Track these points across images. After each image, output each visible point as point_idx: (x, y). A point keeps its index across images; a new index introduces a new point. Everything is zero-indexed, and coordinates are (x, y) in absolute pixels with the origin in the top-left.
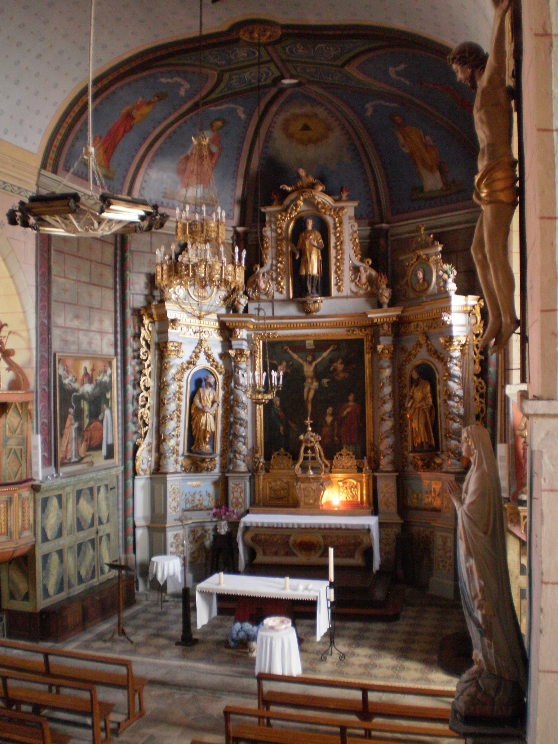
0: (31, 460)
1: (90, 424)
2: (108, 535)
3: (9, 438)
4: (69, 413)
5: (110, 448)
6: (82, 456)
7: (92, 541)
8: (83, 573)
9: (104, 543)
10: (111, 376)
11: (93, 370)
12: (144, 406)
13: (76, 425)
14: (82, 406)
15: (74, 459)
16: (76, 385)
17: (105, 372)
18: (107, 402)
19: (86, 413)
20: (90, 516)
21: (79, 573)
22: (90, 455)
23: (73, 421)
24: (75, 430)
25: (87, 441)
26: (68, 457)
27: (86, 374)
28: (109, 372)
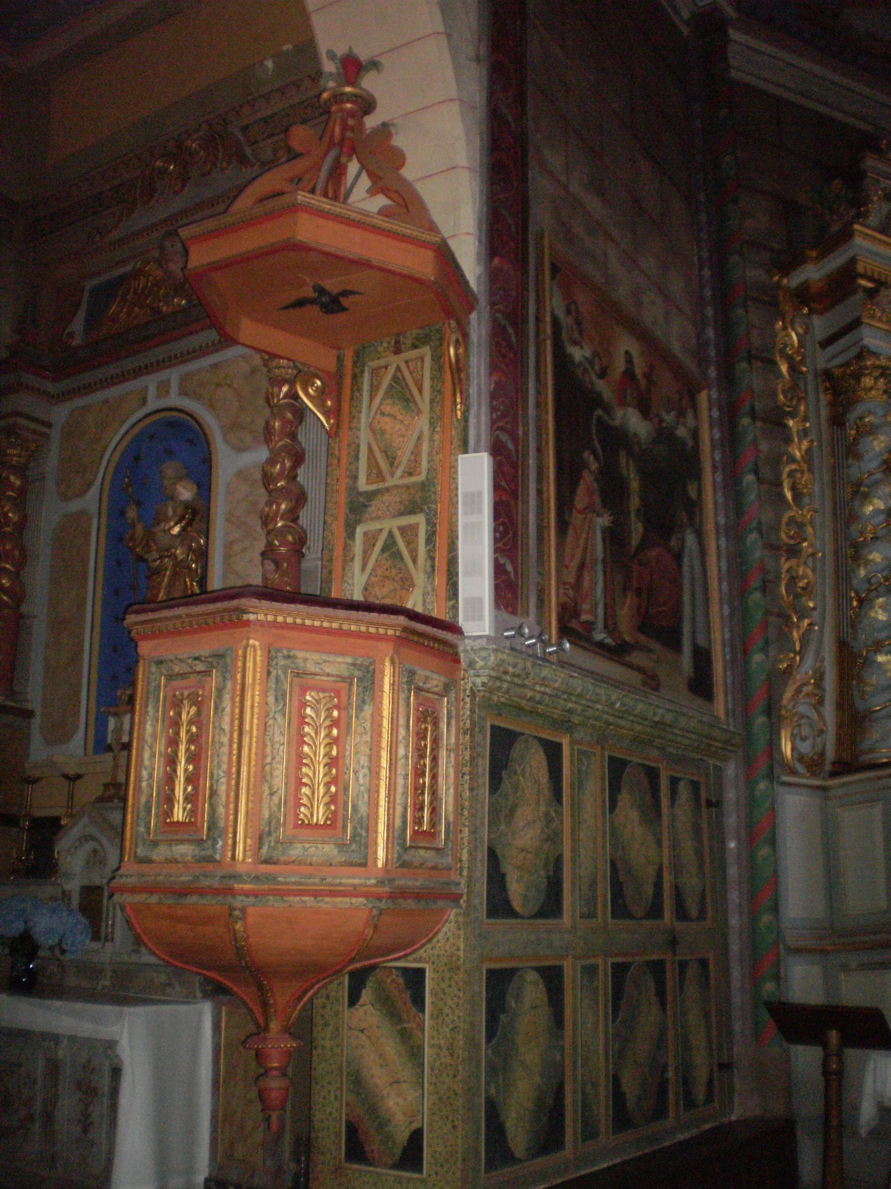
0: (452, 546)
1: (644, 545)
2: (704, 964)
3: (372, 496)
4: (585, 466)
5: (702, 657)
6: (627, 638)
7: (657, 968)
8: (630, 1089)
9: (692, 990)
10: (695, 434)
11: (648, 377)
12: (793, 551)
13: (603, 521)
14: (625, 472)
15: (599, 636)
16: (603, 388)
17: (681, 414)
18: (694, 507)
19: (635, 502)
20: (651, 871)
21: (616, 1082)
22: (650, 651)
23: (597, 500)
24: (604, 531)
25: (638, 592)
26: (585, 617)
27: (629, 374)
28: (690, 420)
